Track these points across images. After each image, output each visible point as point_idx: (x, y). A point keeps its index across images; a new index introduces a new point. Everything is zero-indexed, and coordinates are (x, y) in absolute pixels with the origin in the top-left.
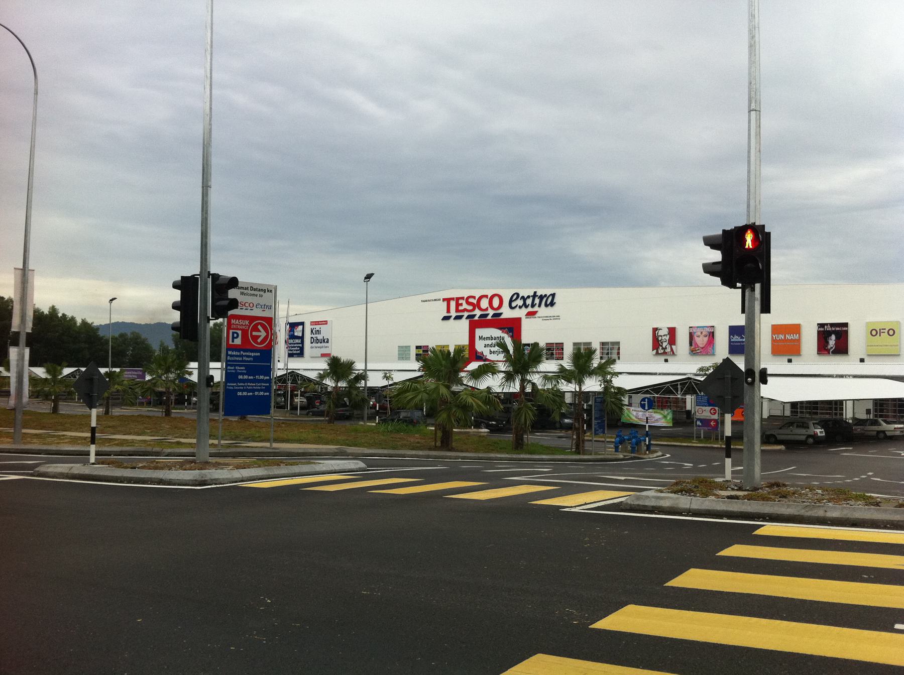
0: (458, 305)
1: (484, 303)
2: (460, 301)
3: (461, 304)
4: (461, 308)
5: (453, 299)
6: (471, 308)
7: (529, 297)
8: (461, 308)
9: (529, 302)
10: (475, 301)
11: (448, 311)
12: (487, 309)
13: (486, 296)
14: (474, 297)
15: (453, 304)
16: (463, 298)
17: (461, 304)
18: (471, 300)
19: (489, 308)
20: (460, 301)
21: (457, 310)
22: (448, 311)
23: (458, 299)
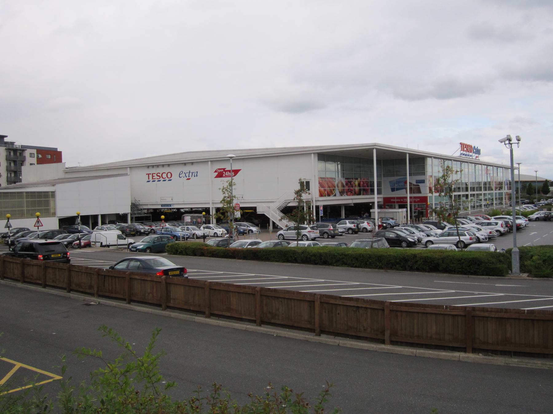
0: (153, 176)
1: (164, 176)
2: (154, 175)
3: (154, 176)
4: (154, 178)
5: (150, 174)
6: (159, 177)
7: (187, 173)
8: (154, 178)
9: (187, 175)
10: (160, 175)
11: (149, 179)
12: (165, 178)
13: (165, 173)
14: (160, 173)
15: (151, 176)
16: (155, 174)
17: (154, 176)
18: (158, 174)
19: (166, 177)
20: (154, 175)
21: (153, 179)
22: (149, 179)
23: (153, 174)
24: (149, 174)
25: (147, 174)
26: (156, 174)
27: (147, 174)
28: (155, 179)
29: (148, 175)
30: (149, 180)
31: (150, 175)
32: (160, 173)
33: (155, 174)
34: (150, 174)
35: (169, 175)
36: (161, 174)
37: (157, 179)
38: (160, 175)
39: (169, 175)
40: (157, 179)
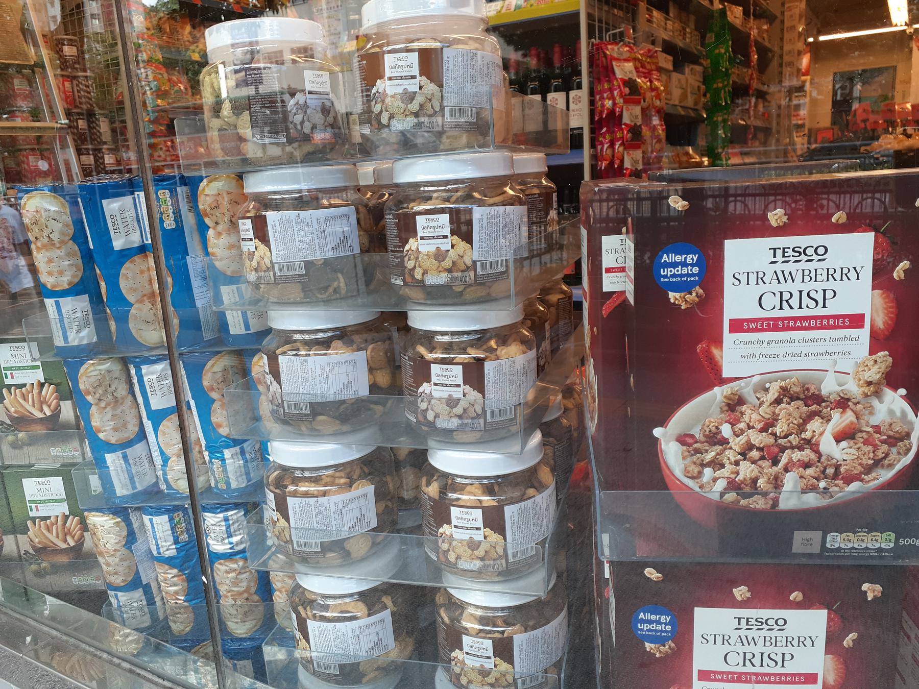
2: (786, 250)
4: (786, 254)
5: (780, 249)
6: (798, 254)
11: (775, 256)
14: (800, 248)
16: (789, 248)
18: (796, 249)
20: (786, 250)
21: (784, 256)
24: (775, 249)
28: (789, 256)
32: (800, 248)
33: (789, 248)
34: (780, 249)
38: (802, 250)
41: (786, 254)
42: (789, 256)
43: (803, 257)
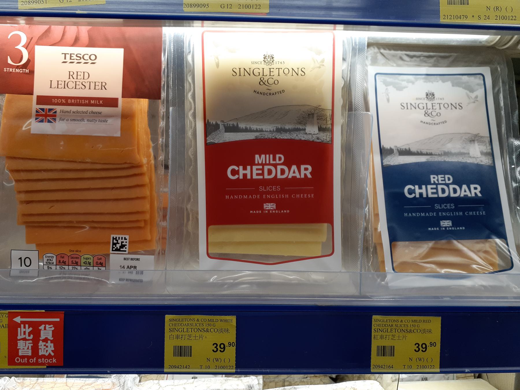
0: (71, 56)
1: (86, 57)
2: (72, 55)
3: (73, 57)
5: (68, 54)
6: (79, 58)
8: (72, 58)
10: (81, 56)
11: (65, 59)
12: (87, 60)
13: (88, 54)
14: (81, 54)
15: (68, 56)
16: (74, 54)
17: (73, 57)
18: (78, 55)
19: (89, 59)
21: (71, 59)
22: (65, 59)
23: (71, 54)
24: (65, 54)
25: (62, 54)
26: (75, 54)
27: (62, 54)
28: (74, 59)
29: (64, 55)
30: (65, 61)
31: (67, 55)
32: (81, 54)
33: (74, 54)
34: (68, 54)
35: (93, 57)
36: (82, 55)
37: (76, 59)
38: (81, 56)
39: (93, 57)
40: (76, 59)
41: (72, 58)
42: (74, 59)
43: (82, 61)
